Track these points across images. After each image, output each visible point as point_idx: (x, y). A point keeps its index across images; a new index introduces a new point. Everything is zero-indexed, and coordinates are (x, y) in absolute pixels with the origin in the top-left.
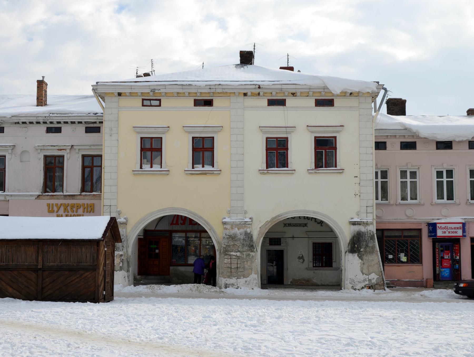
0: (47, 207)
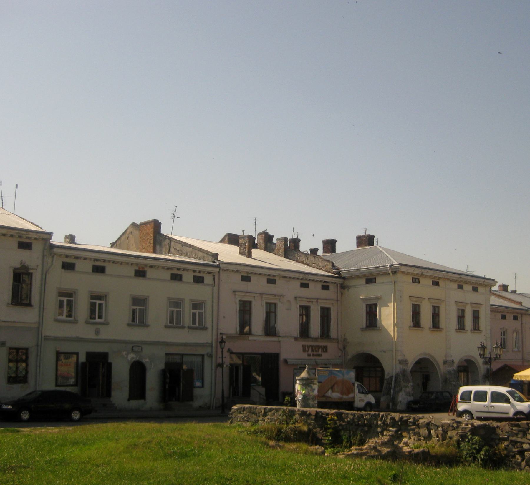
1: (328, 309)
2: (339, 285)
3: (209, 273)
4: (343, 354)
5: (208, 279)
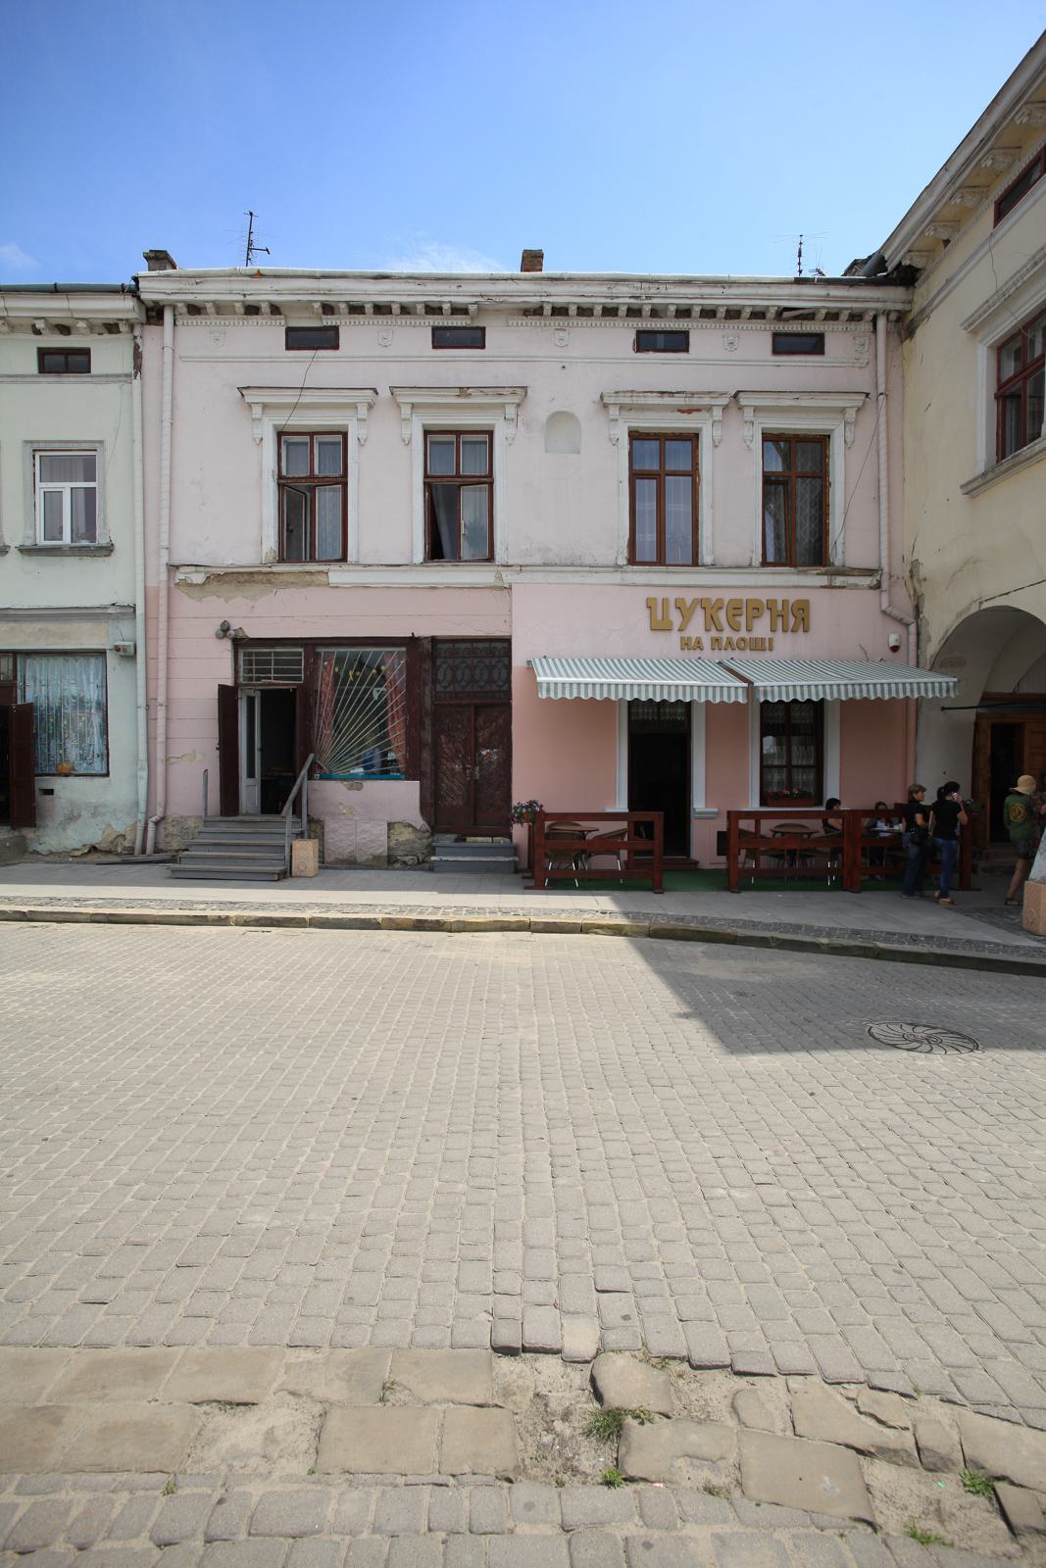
0: (647, 612)
1: (820, 442)
2: (881, 323)
3: (112, 328)
4: (913, 639)
5: (110, 355)
